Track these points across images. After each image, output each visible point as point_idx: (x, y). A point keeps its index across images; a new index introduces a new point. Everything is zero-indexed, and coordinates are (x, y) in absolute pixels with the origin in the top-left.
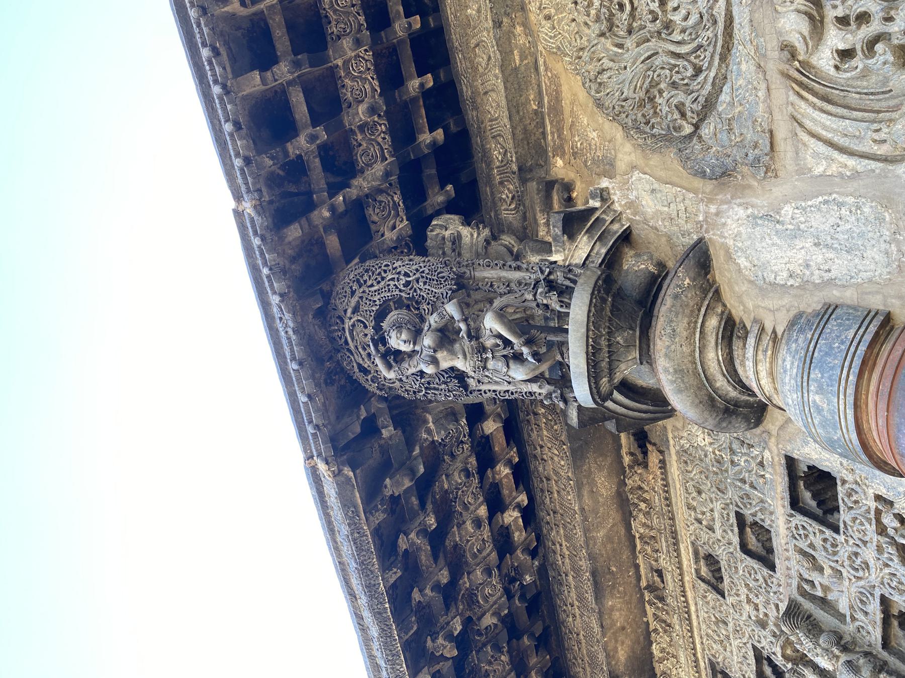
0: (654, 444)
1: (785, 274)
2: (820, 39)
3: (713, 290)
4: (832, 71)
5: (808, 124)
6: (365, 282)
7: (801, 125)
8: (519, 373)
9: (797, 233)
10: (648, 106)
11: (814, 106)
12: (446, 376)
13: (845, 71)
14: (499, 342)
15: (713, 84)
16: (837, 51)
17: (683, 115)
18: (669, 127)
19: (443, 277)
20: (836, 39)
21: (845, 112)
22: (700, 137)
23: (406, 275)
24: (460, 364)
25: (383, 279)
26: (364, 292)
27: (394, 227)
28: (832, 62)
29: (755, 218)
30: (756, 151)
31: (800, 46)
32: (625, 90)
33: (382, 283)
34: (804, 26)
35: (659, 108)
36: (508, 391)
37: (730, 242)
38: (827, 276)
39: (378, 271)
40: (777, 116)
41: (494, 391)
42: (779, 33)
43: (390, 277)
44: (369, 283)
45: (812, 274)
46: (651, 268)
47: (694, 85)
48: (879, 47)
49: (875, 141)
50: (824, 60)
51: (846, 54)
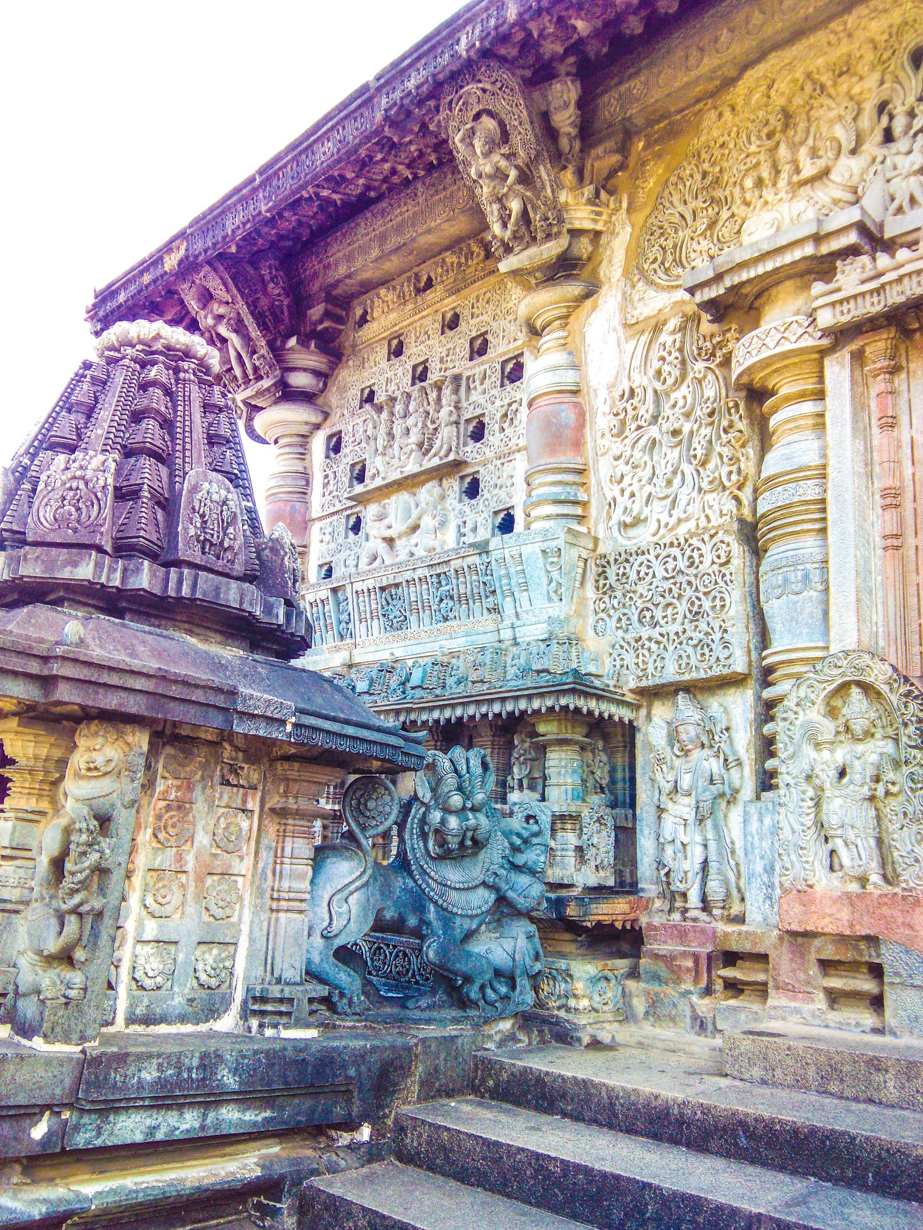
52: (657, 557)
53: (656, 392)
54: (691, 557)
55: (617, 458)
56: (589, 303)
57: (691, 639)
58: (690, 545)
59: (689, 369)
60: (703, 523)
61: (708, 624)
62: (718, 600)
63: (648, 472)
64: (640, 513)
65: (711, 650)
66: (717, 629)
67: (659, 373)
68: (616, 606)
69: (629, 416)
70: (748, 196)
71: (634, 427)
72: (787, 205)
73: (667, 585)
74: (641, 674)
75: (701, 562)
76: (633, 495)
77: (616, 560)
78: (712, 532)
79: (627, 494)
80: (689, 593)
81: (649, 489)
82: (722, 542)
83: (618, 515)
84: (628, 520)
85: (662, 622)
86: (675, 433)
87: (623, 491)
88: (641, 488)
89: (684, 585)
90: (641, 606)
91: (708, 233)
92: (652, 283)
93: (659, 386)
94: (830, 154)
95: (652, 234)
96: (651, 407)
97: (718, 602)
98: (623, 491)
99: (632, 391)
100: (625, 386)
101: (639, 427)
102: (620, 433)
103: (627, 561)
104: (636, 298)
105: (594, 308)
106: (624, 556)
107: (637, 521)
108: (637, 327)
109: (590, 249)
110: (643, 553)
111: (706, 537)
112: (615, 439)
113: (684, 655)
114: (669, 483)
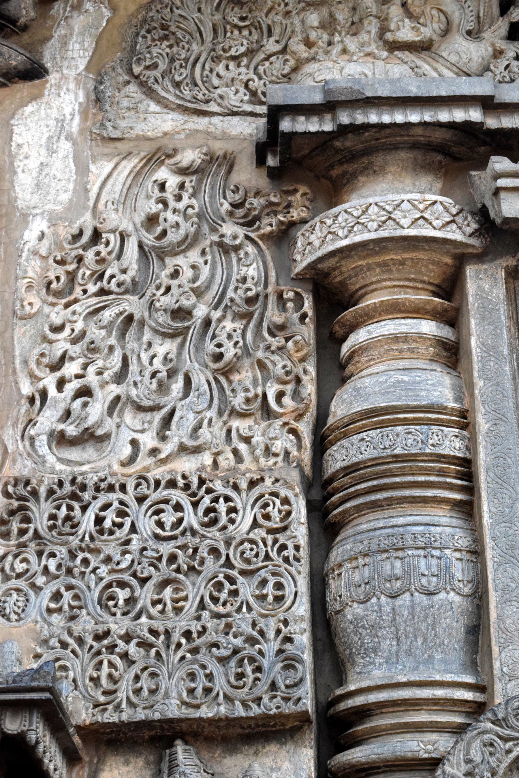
1: (20, 142)
2: (175, 172)
3: (6, 82)
4: (154, 178)
5: (124, 163)
7: (124, 158)
9: (51, 151)
10: (162, 32)
11: (135, 167)
13: (153, 186)
15: (164, 98)
16: (166, 182)
17: (147, 68)
18: (141, 53)
20: (173, 181)
21: (127, 186)
22: (128, 82)
28: (159, 179)
29: (63, 121)
30: (111, 128)
31: (172, 161)
32: (179, 12)
34: (185, 163)
35: (159, 43)
37: (45, 100)
38: (19, 170)
40: (132, 144)
42: (184, 149)
45: (21, 161)
46: (22, 20)
47: (167, 83)
48: (160, 206)
49: (107, 202)
50: (163, 173)
51: (162, 187)
52: (141, 500)
53: (141, 246)
54: (208, 511)
55: (58, 329)
56: (24, 88)
57: (216, 645)
58: (209, 491)
59: (205, 228)
60: (227, 460)
61: (254, 625)
62: (270, 586)
63: (115, 362)
64: (99, 424)
65: (259, 669)
66: (271, 634)
67: (152, 220)
68: (52, 568)
69: (85, 272)
70: (313, 35)
71: (92, 288)
72: (380, 64)
73: (166, 549)
74: (102, 699)
75: (232, 521)
76: (85, 392)
77: (51, 492)
78: (256, 477)
79: (71, 388)
80: (211, 566)
81: (114, 390)
82: (275, 494)
83: (48, 420)
84: (71, 430)
85: (154, 611)
86: (181, 313)
87: (61, 384)
88: (103, 385)
89: (203, 552)
90: (108, 579)
91: (245, 61)
92: (150, 93)
93: (149, 239)
94: (436, 26)
95: (149, 31)
96: (135, 266)
97: (269, 589)
98: (61, 384)
99: (97, 235)
100: (87, 222)
101: (102, 292)
102: (61, 291)
103: (74, 496)
104: (125, 103)
105: (35, 97)
106: (68, 488)
107: (90, 437)
108: (119, 145)
109: (32, 14)
110: (111, 488)
111: (244, 485)
112: (51, 299)
113: (201, 673)
114: (163, 388)
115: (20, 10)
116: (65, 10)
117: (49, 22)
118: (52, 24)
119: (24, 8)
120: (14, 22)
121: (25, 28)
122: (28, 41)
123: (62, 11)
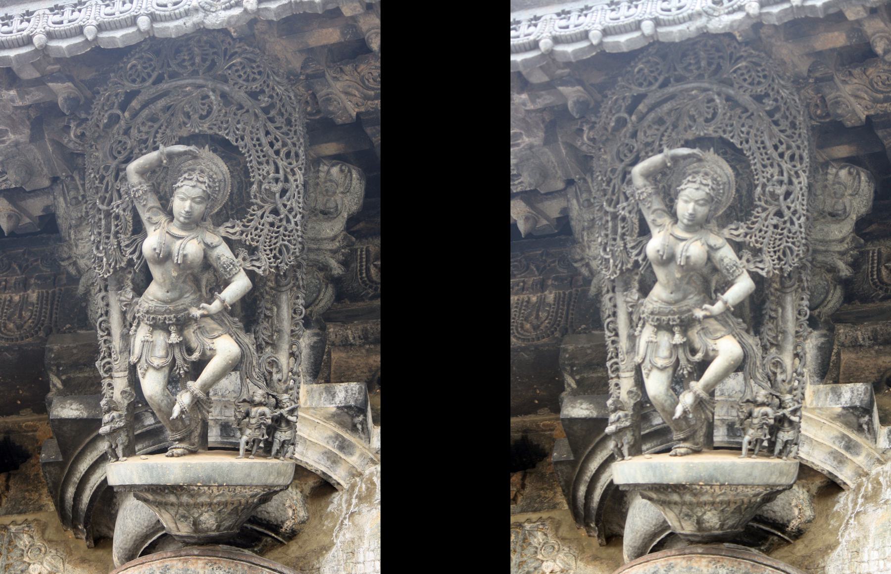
0: (7, 488)
6: (272, 120)
8: (152, 385)
12: (135, 257)
14: (196, 356)
19: (280, 252)
23: (284, 192)
24: (155, 291)
25: (277, 153)
26: (256, 115)
27: (347, 93)
33: (271, 152)
36: (109, 334)
39: (289, 142)
41: (107, 313)
43: (281, 164)
44: (271, 127)
109: (302, 514)
115: (285, 510)
116: (350, 504)
117: (328, 523)
118: (331, 525)
119: (290, 507)
120: (275, 527)
121: (293, 535)
122: (298, 554)
123: (344, 506)
